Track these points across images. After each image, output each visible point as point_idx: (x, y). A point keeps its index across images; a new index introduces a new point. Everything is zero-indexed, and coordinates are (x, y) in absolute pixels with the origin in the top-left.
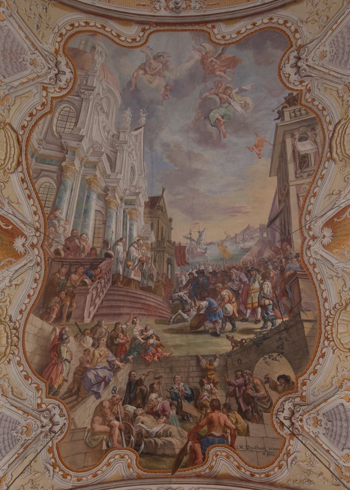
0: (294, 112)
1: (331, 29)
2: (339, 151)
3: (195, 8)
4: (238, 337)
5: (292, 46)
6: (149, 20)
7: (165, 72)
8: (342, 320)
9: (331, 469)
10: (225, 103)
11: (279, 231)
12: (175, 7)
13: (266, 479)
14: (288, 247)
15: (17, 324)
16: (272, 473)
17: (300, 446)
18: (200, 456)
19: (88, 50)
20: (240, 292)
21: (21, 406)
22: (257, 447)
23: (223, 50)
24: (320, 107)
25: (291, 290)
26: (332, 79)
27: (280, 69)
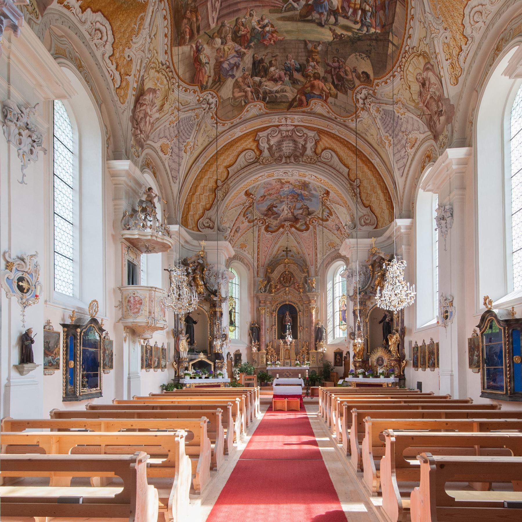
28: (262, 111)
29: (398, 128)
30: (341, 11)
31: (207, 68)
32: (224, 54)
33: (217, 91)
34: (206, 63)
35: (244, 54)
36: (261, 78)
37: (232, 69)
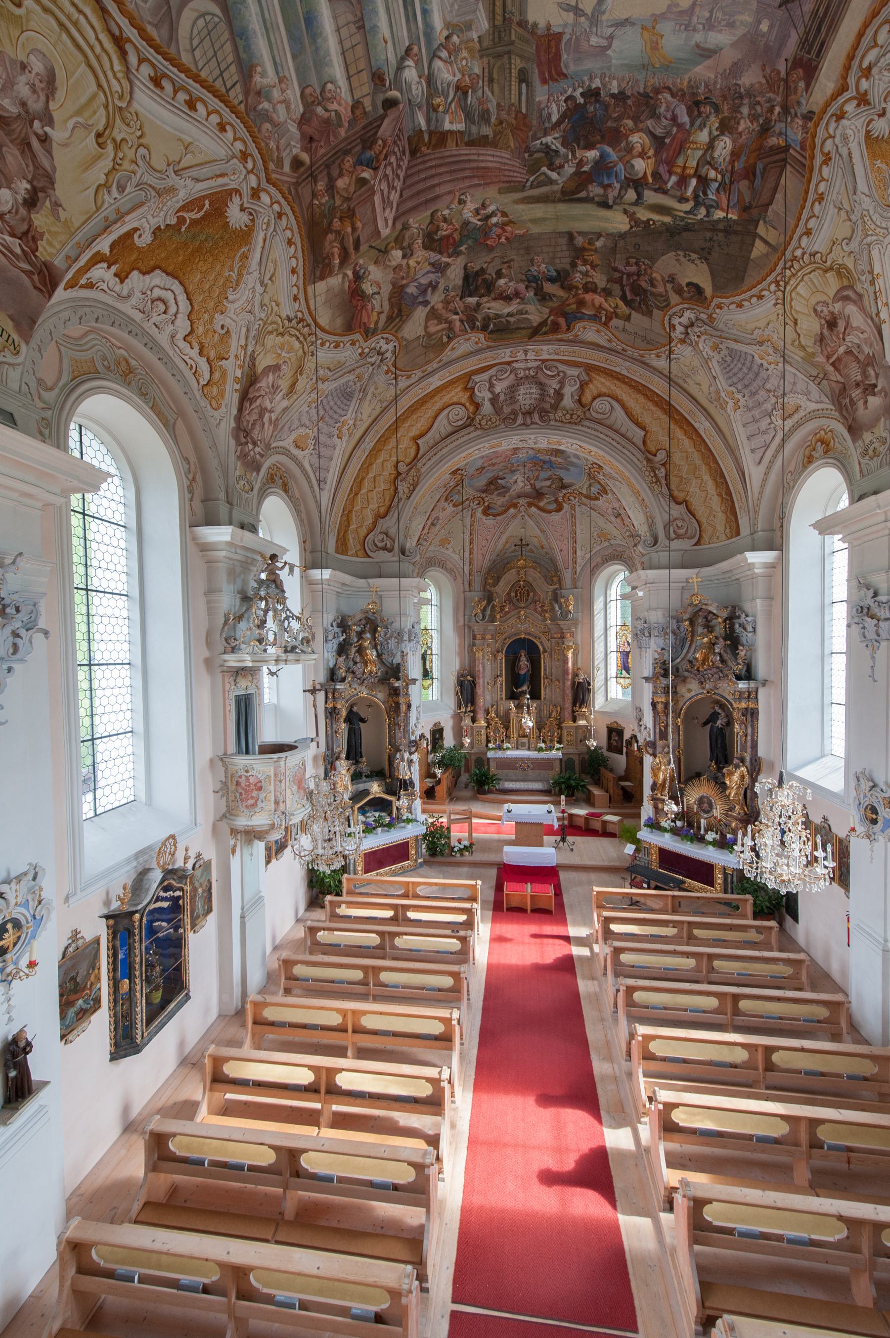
4: (643, 215)
14: (802, 84)
30: (650, 180)
32: (408, 272)
35: (448, 265)
37: (424, 292)
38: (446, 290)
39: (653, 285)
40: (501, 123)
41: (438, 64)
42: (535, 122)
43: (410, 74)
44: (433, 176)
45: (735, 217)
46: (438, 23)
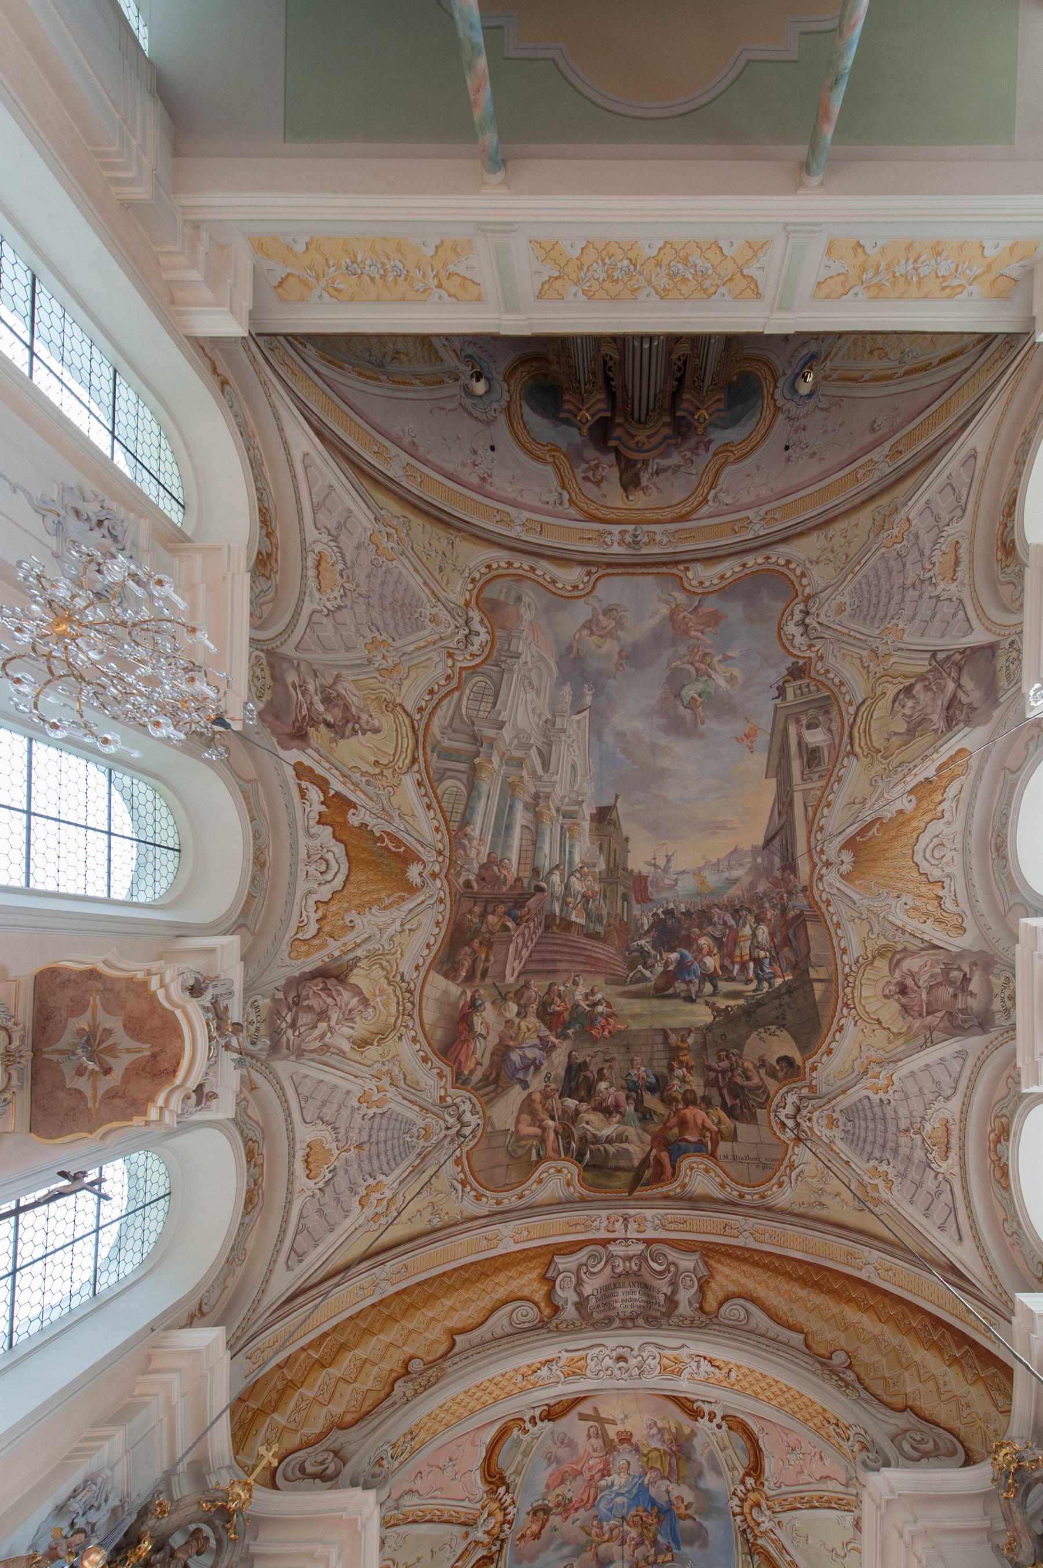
0: (800, 688)
1: (852, 572)
2: (863, 743)
3: (661, 542)
5: (797, 596)
6: (597, 559)
7: (619, 632)
8: (868, 979)
9: (852, 1188)
10: (702, 676)
11: (779, 854)
12: (634, 542)
13: (759, 1202)
15: (412, 985)
16: (769, 1193)
17: (808, 1156)
18: (669, 1170)
19: (511, 601)
20: (724, 940)
21: (417, 1099)
22: (747, 1157)
23: (700, 601)
24: (836, 681)
25: (795, 937)
26: (853, 642)
27: (780, 628)
28: (572, 1189)
29: (892, 1128)
31: (480, 1045)
33: (487, 1103)
34: (480, 1035)
36: (580, 1102)
38: (548, 1077)
39: (748, 1078)
40: (610, 925)
41: (573, 879)
42: (633, 929)
43: (556, 878)
44: (556, 952)
45: (790, 978)
46: (577, 859)
